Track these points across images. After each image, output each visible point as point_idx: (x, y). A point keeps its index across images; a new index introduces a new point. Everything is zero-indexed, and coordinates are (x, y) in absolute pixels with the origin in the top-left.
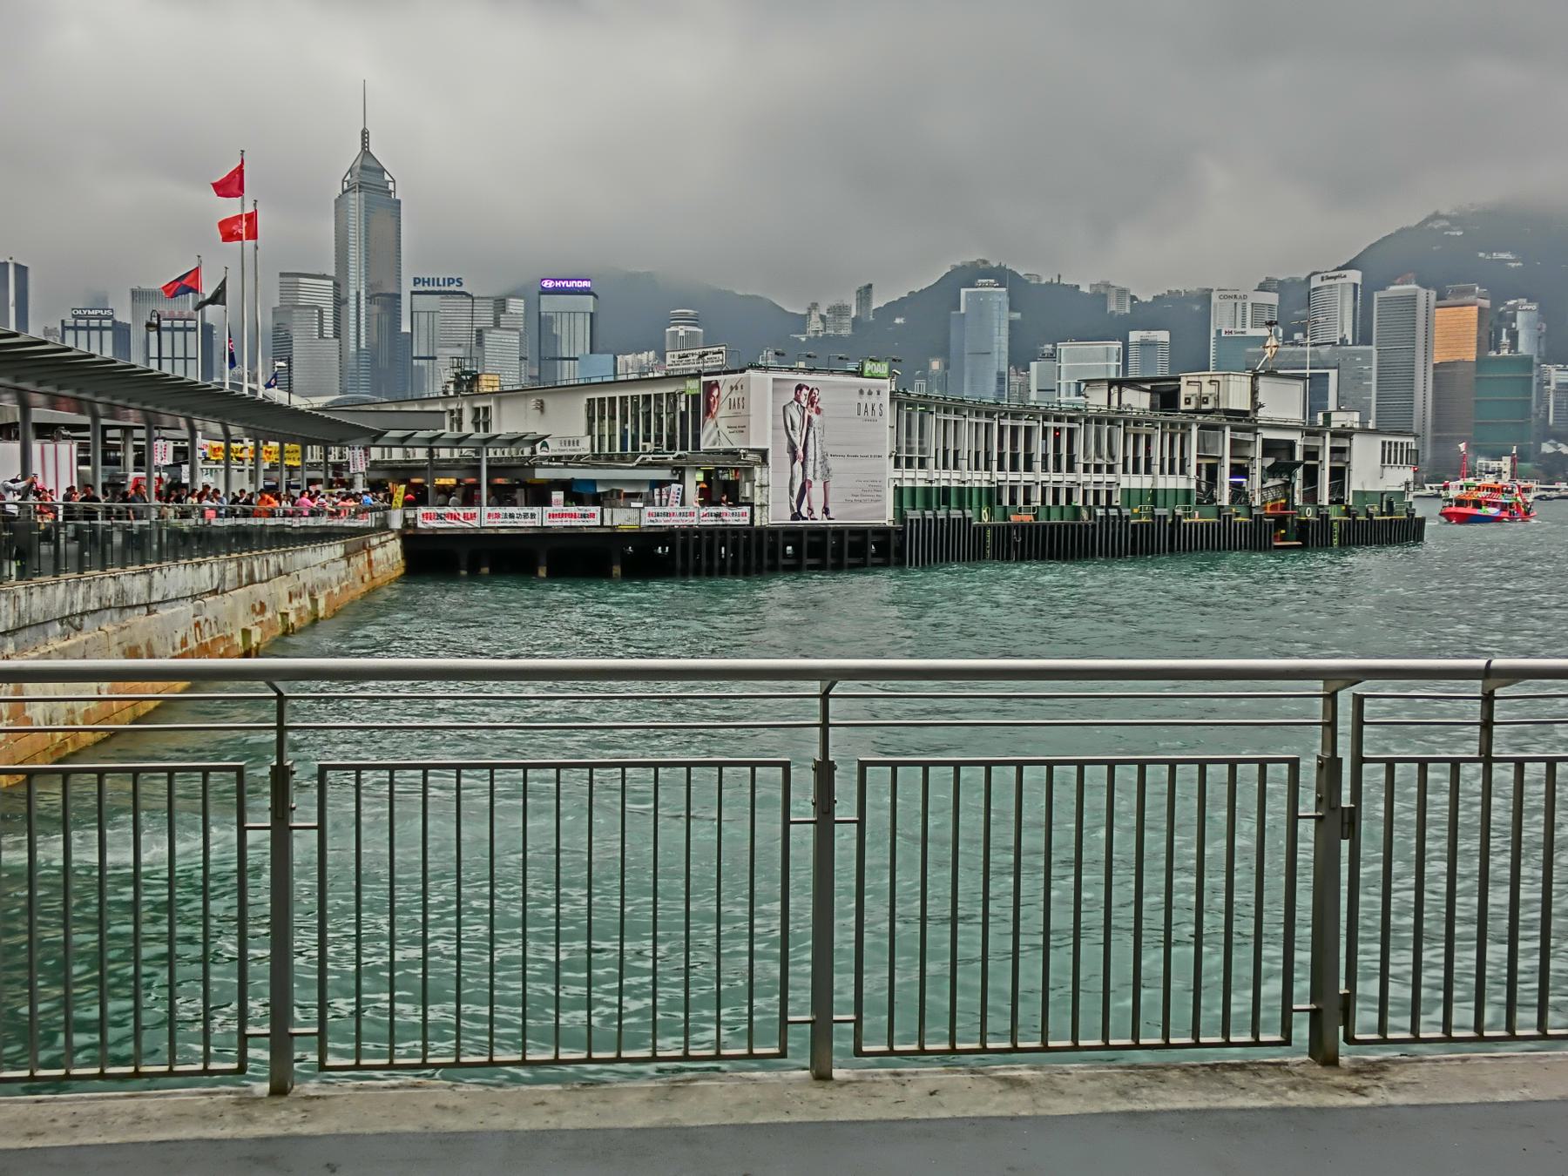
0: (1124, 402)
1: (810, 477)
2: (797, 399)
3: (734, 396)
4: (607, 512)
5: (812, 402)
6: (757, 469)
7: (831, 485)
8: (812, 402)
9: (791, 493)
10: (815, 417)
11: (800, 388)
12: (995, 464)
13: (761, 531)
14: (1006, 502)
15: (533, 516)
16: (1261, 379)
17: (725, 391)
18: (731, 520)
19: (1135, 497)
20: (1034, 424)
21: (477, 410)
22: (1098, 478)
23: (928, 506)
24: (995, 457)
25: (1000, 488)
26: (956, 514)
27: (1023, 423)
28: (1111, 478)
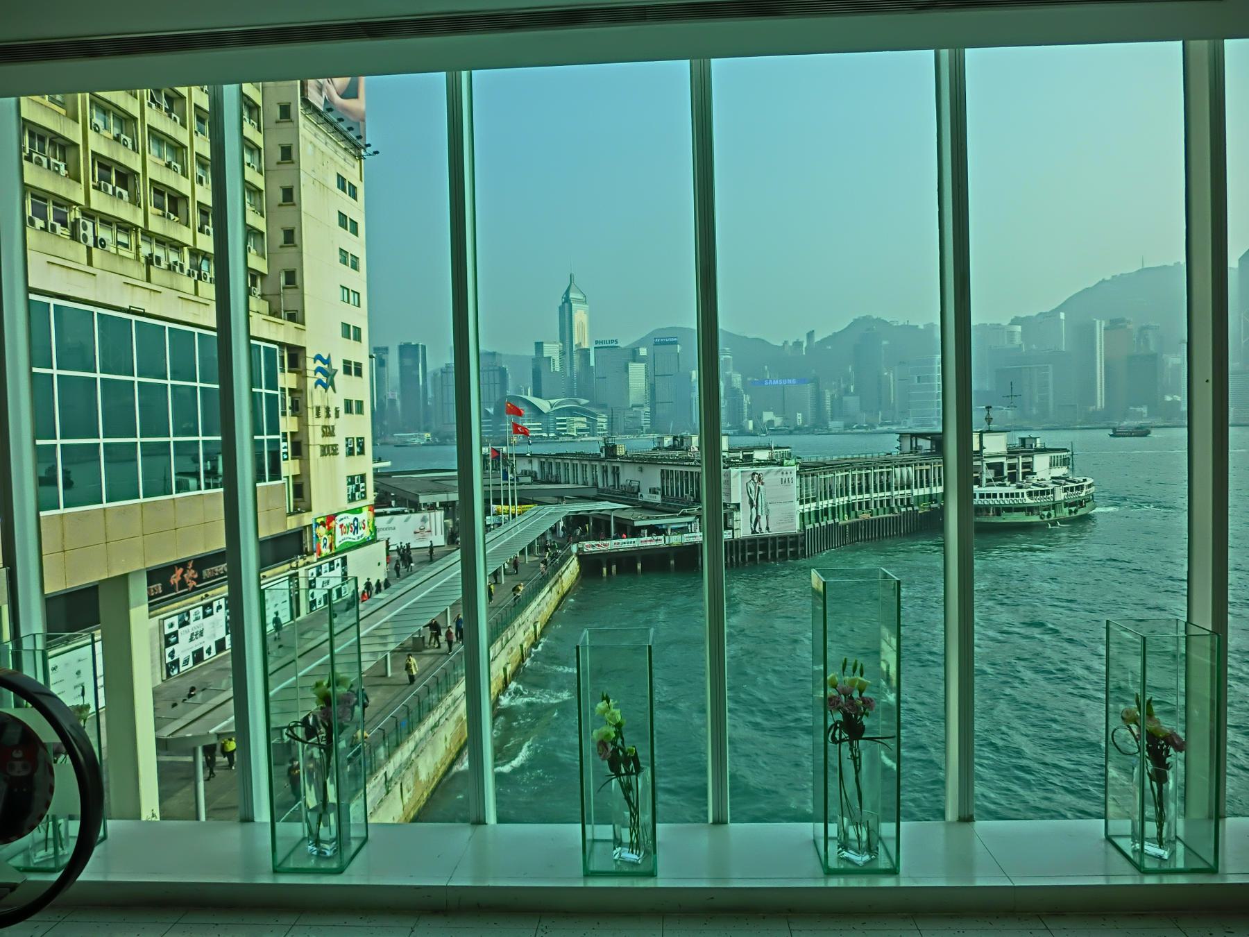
0: (919, 444)
1: (760, 514)
2: (753, 479)
4: (667, 537)
5: (759, 479)
6: (735, 513)
7: (770, 517)
8: (759, 479)
9: (751, 522)
10: (761, 486)
11: (754, 474)
12: (850, 493)
13: (737, 542)
14: (857, 509)
19: (920, 498)
20: (869, 471)
21: (614, 467)
22: (902, 492)
24: (850, 489)
25: (853, 504)
26: (831, 522)
27: (864, 472)
28: (908, 491)
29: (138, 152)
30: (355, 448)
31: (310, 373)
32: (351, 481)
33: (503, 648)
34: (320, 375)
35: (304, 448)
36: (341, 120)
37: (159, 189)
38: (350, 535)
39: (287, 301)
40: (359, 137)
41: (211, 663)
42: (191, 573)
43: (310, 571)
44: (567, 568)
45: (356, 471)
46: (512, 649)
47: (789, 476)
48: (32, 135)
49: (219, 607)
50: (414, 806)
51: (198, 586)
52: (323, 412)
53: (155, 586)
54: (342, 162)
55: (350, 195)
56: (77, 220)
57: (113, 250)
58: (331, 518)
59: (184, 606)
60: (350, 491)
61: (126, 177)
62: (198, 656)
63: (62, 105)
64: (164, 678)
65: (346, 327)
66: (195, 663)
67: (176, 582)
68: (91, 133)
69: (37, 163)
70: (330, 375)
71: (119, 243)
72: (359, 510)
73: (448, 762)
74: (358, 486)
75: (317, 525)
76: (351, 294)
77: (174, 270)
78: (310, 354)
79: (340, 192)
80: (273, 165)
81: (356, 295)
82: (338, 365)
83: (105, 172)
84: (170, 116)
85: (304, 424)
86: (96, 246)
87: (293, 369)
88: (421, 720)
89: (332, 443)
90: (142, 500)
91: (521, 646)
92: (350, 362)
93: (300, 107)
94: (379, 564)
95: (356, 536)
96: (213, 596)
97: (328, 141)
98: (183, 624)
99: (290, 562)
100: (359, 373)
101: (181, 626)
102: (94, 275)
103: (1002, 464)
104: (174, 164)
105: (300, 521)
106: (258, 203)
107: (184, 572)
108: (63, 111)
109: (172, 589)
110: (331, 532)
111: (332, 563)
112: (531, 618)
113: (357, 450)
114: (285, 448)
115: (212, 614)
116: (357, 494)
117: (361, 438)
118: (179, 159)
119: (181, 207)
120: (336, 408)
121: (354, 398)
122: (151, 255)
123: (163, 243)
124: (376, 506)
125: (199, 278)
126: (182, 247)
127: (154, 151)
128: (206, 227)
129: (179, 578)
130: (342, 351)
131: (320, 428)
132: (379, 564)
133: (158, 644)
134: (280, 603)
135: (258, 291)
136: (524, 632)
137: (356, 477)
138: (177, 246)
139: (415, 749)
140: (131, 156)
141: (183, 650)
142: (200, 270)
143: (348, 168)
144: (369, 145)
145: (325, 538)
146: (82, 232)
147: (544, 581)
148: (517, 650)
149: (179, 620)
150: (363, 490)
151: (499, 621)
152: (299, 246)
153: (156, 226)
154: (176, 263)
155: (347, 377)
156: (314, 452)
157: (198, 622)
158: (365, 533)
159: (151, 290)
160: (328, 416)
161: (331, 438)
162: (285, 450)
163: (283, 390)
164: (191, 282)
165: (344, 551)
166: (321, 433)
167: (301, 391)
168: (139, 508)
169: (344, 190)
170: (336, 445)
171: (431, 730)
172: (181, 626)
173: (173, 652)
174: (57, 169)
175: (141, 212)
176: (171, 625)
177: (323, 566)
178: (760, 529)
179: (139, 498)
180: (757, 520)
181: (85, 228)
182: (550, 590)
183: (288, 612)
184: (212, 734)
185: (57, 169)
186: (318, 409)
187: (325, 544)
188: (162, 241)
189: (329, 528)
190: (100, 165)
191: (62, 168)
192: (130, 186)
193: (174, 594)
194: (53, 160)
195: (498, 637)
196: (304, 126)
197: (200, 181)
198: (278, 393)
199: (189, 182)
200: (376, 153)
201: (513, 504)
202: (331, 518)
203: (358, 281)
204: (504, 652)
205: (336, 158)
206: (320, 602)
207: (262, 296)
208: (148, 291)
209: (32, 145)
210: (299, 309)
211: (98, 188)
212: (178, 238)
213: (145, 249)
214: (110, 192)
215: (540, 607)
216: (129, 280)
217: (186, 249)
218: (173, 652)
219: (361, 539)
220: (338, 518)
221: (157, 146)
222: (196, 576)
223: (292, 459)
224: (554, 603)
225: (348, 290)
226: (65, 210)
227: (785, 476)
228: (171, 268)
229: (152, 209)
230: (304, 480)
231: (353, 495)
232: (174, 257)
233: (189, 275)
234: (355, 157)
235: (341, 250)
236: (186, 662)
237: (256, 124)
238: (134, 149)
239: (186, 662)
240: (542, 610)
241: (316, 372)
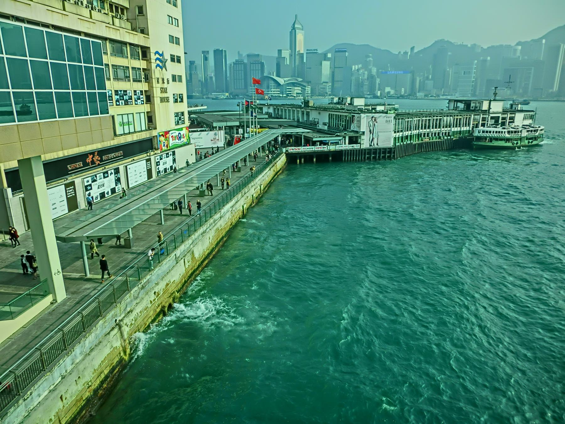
3: (358, 119)
4: (328, 147)
5: (375, 120)
6: (362, 136)
7: (379, 139)
8: (375, 120)
10: (376, 124)
11: (372, 117)
12: (420, 128)
13: (362, 150)
16: (492, 102)
17: (356, 118)
18: (356, 147)
20: (431, 118)
22: (446, 129)
23: (402, 141)
24: (420, 127)
26: (409, 142)
28: (449, 129)
30: (178, 99)
31: (153, 61)
32: (177, 115)
34: (158, 62)
38: (177, 141)
39: (140, 23)
42: (97, 157)
43: (157, 158)
45: (179, 110)
46: (247, 197)
47: (390, 119)
49: (111, 173)
50: (192, 269)
52: (160, 81)
58: (167, 133)
62: (102, 195)
65: (171, 37)
66: (101, 198)
70: (164, 62)
72: (181, 129)
73: (211, 249)
74: (180, 118)
75: (160, 136)
76: (174, 20)
77: (78, 4)
78: (153, 50)
81: (176, 21)
82: (167, 57)
85: (151, 86)
91: (253, 196)
92: (174, 56)
95: (180, 141)
98: (94, 181)
99: (147, 153)
100: (179, 61)
101: (92, 182)
102: (30, 5)
103: (499, 117)
105: (150, 134)
109: (88, 165)
111: (168, 154)
113: (179, 100)
114: (142, 98)
115: (108, 176)
116: (180, 121)
120: (167, 79)
121: (177, 74)
124: (190, 127)
130: (169, 50)
131: (159, 89)
134: (142, 172)
139: (192, 243)
142: (92, 4)
147: (268, 164)
148: (250, 198)
149: (92, 179)
151: (241, 184)
156: (157, 101)
157: (101, 180)
158: (184, 140)
159: (62, 14)
160: (163, 83)
161: (165, 94)
162: (142, 99)
163: (107, 65)
164: (88, 10)
165: (174, 148)
167: (149, 70)
170: (168, 97)
172: (92, 182)
173: (90, 193)
176: (88, 181)
178: (374, 144)
180: (372, 140)
182: (270, 169)
184: (84, 237)
186: (158, 79)
187: (164, 145)
189: (166, 138)
198: (104, 67)
204: (243, 198)
207: (127, 20)
208: (61, 15)
216: (50, 8)
218: (90, 193)
220: (170, 132)
222: (99, 159)
224: (272, 176)
225: (172, 17)
227: (388, 119)
230: (152, 114)
231: (178, 122)
241: (156, 60)
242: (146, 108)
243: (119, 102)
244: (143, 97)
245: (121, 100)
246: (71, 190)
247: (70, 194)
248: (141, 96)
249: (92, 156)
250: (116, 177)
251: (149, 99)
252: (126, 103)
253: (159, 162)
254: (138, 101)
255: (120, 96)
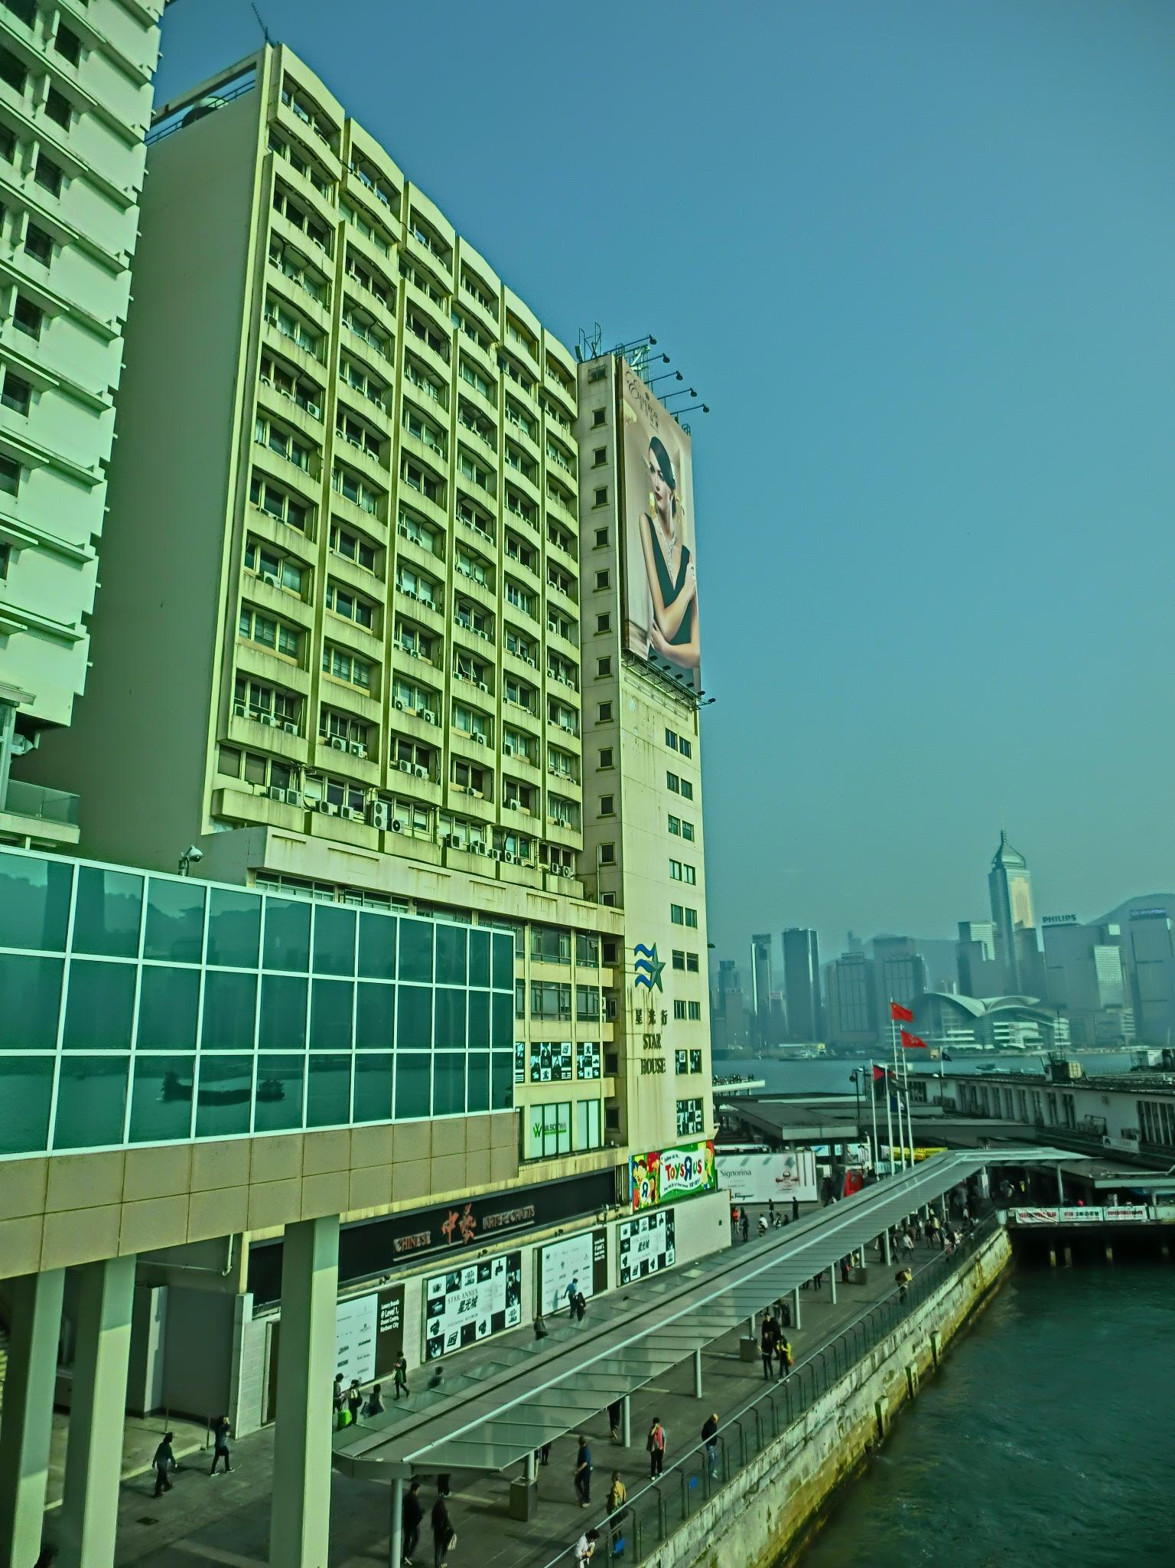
15: (1097, 1214)
21: (1065, 1096)
29: (441, 727)
30: (689, 1063)
31: (629, 968)
32: (683, 1106)
33: (875, 1370)
34: (641, 970)
35: (620, 1062)
36: (667, 668)
37: (462, 763)
38: (681, 1180)
39: (605, 881)
40: (691, 685)
41: (484, 1345)
42: (468, 1221)
44: (989, 1248)
45: (690, 1094)
46: (891, 1373)
48: (334, 719)
49: (499, 1269)
51: (476, 1238)
52: (645, 1017)
53: (422, 1234)
54: (672, 716)
55: (681, 752)
56: (372, 802)
57: (409, 833)
58: (654, 1156)
59: (456, 1264)
60: (681, 1120)
61: (427, 754)
62: (468, 1333)
63: (367, 686)
64: (424, 1360)
66: (464, 1342)
67: (449, 1231)
68: (392, 711)
69: (335, 747)
70: (655, 969)
71: (415, 825)
72: (693, 1147)
74: (692, 1115)
75: (635, 1164)
76: (684, 869)
78: (630, 943)
79: (669, 749)
80: (590, 726)
81: (690, 870)
82: (665, 957)
83: (405, 750)
84: (478, 686)
85: (620, 1032)
86: (389, 829)
87: (610, 963)
88: (725, 1480)
89: (656, 1057)
90: (304, 1129)
91: (908, 1369)
93: (620, 660)
94: (720, 1223)
95: (689, 1182)
96: (493, 1252)
97: (655, 693)
98: (453, 1287)
99: (597, 1213)
100: (694, 966)
101: (449, 1290)
102: (377, 860)
104: (479, 735)
106: (574, 770)
107: (459, 1219)
108: (367, 693)
110: (653, 1174)
111: (653, 1218)
112: (927, 1325)
113: (690, 1065)
114: (596, 1062)
115: (489, 1277)
117: (696, 1051)
118: (486, 731)
119: (485, 783)
120: (663, 1012)
122: (449, 836)
123: (464, 822)
124: (719, 1139)
125: (502, 859)
126: (485, 825)
127: (460, 724)
128: (512, 801)
129: (453, 1226)
130: (671, 939)
131: (642, 1037)
132: (720, 1223)
133: (420, 1312)
135: (571, 871)
136: (914, 1348)
137: (690, 1103)
138: (479, 824)
139: (714, 1526)
140: (432, 730)
141: (450, 1323)
142: (503, 849)
143: (681, 721)
144: (703, 693)
145: (645, 1183)
146: (376, 815)
149: (448, 1282)
150: (699, 1120)
151: (869, 1326)
152: (618, 815)
153: (455, 803)
154: (476, 843)
155: (678, 971)
156: (633, 1068)
158: (701, 1179)
159: (438, 874)
160: (652, 1022)
161: (656, 1051)
162: (597, 1065)
165: (671, 1202)
166: (642, 1043)
167: (618, 991)
168: (301, 1137)
169: (674, 747)
170: (662, 1060)
171: (744, 1497)
172: (449, 1290)
173: (437, 1324)
174: (355, 751)
175: (439, 790)
176: (437, 1288)
177: (641, 1221)
179: (301, 1127)
181: (379, 812)
182: (960, 1281)
183: (590, 1282)
185: (355, 751)
186: (639, 1012)
187: (645, 1192)
188: (463, 820)
189: (651, 1169)
190: (401, 744)
191: (361, 749)
192: (431, 764)
193: (445, 1246)
194: (352, 743)
195: (866, 1352)
196: (625, 679)
197: (508, 750)
199: (495, 753)
200: (712, 700)
201: (907, 1145)
202: (654, 1156)
203: (693, 853)
204: (877, 1378)
205: (664, 710)
206: (635, 1271)
207: (577, 876)
208: (436, 876)
209: (333, 730)
210: (617, 889)
211: (395, 768)
212: (480, 816)
213: (444, 829)
214: (409, 770)
215: (942, 1308)
216: (415, 864)
217: (489, 826)
218: (437, 1324)
219: (695, 1186)
220: (664, 1156)
221: (463, 717)
222: (474, 1225)
223: (605, 1076)
224: (967, 1304)
225: (680, 864)
226: (361, 793)
228: (470, 849)
229: (453, 786)
230: (619, 1104)
231: (686, 1126)
232: (475, 836)
233: (490, 856)
234: (688, 708)
235: (670, 817)
236: (453, 1340)
237: (573, 684)
238: (436, 724)
239: (453, 1340)
240: (947, 1312)
242: (605, 1087)
243: (539, 1073)
244: (599, 1060)
245: (543, 1066)
246: (392, 1312)
247: (387, 1321)
248: (595, 1058)
249: (456, 1215)
250: (511, 1279)
251: (613, 1064)
252: (557, 1074)
253: (628, 1241)
254: (587, 1069)
255: (543, 1058)
